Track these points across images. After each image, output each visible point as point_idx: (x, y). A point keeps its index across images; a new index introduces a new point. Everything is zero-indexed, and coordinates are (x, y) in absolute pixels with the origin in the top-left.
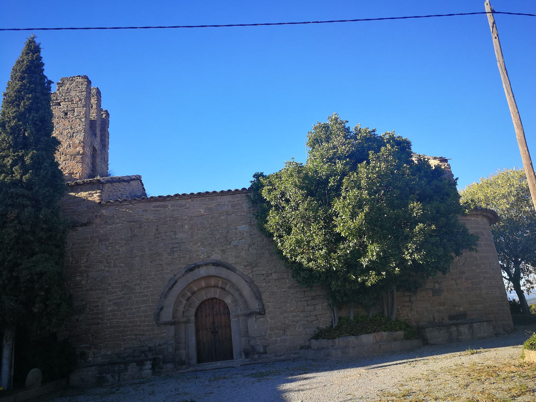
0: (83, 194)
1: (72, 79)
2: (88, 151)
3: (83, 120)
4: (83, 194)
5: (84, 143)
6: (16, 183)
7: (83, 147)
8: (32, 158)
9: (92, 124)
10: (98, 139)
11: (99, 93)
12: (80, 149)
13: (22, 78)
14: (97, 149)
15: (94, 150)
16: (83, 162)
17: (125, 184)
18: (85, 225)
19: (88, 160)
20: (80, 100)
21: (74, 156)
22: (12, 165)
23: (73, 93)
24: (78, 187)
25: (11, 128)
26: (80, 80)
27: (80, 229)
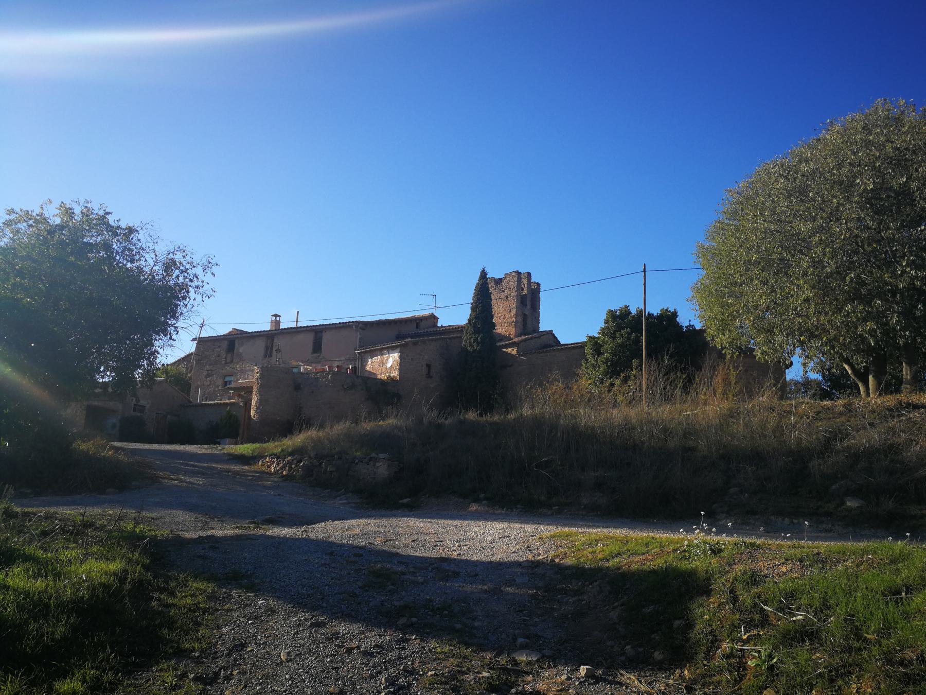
0: (509, 350)
1: (510, 274)
2: (520, 319)
3: (516, 300)
4: (509, 350)
5: (516, 315)
6: (475, 351)
7: (516, 318)
8: (480, 338)
9: (522, 300)
10: (529, 307)
11: (529, 274)
12: (514, 319)
13: (478, 295)
14: (527, 313)
15: (525, 315)
16: (516, 327)
17: (536, 339)
18: (510, 366)
19: (520, 325)
20: (514, 287)
21: (511, 324)
22: (474, 342)
23: (510, 284)
24: (507, 346)
25: (473, 323)
26: (514, 274)
27: (508, 368)
